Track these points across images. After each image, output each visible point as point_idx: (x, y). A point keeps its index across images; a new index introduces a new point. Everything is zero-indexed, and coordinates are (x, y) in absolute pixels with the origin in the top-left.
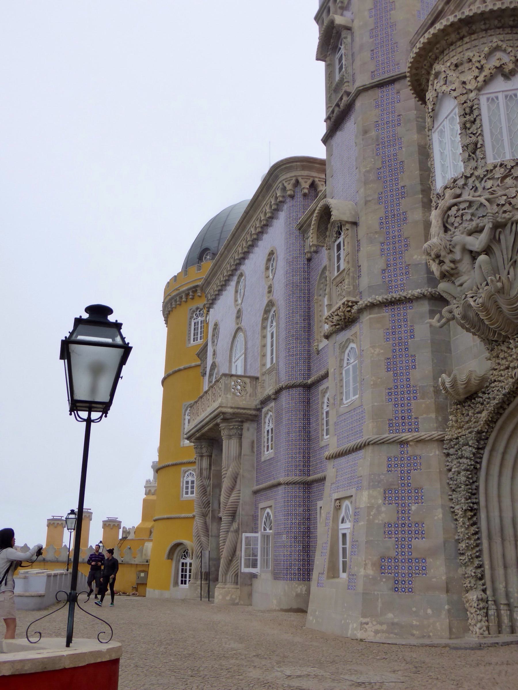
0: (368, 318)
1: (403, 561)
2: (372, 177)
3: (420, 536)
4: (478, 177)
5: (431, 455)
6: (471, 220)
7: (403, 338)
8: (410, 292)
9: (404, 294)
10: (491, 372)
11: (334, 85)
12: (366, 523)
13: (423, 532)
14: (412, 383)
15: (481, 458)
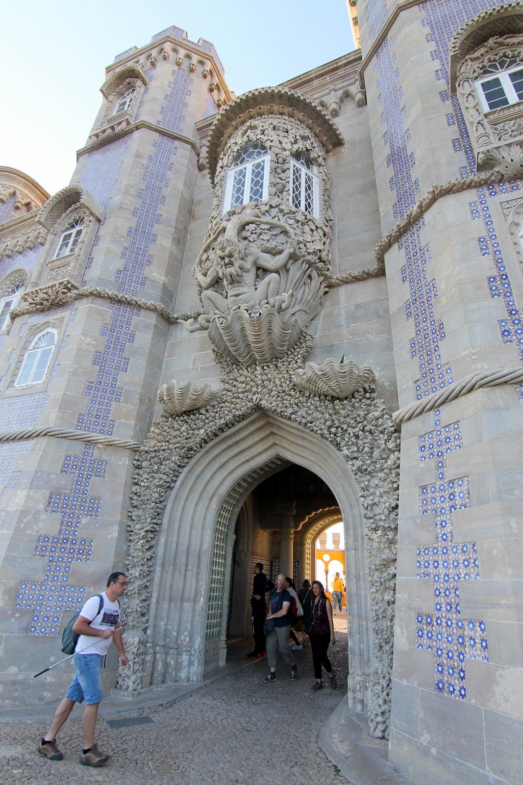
0: (89, 305)
1: (53, 588)
2: (132, 191)
3: (84, 556)
4: (281, 211)
5: (120, 463)
6: (268, 241)
7: (121, 338)
8: (143, 300)
9: (137, 299)
10: (225, 392)
11: (110, 117)
12: (12, 532)
13: (90, 552)
14: (118, 384)
15: (177, 477)
